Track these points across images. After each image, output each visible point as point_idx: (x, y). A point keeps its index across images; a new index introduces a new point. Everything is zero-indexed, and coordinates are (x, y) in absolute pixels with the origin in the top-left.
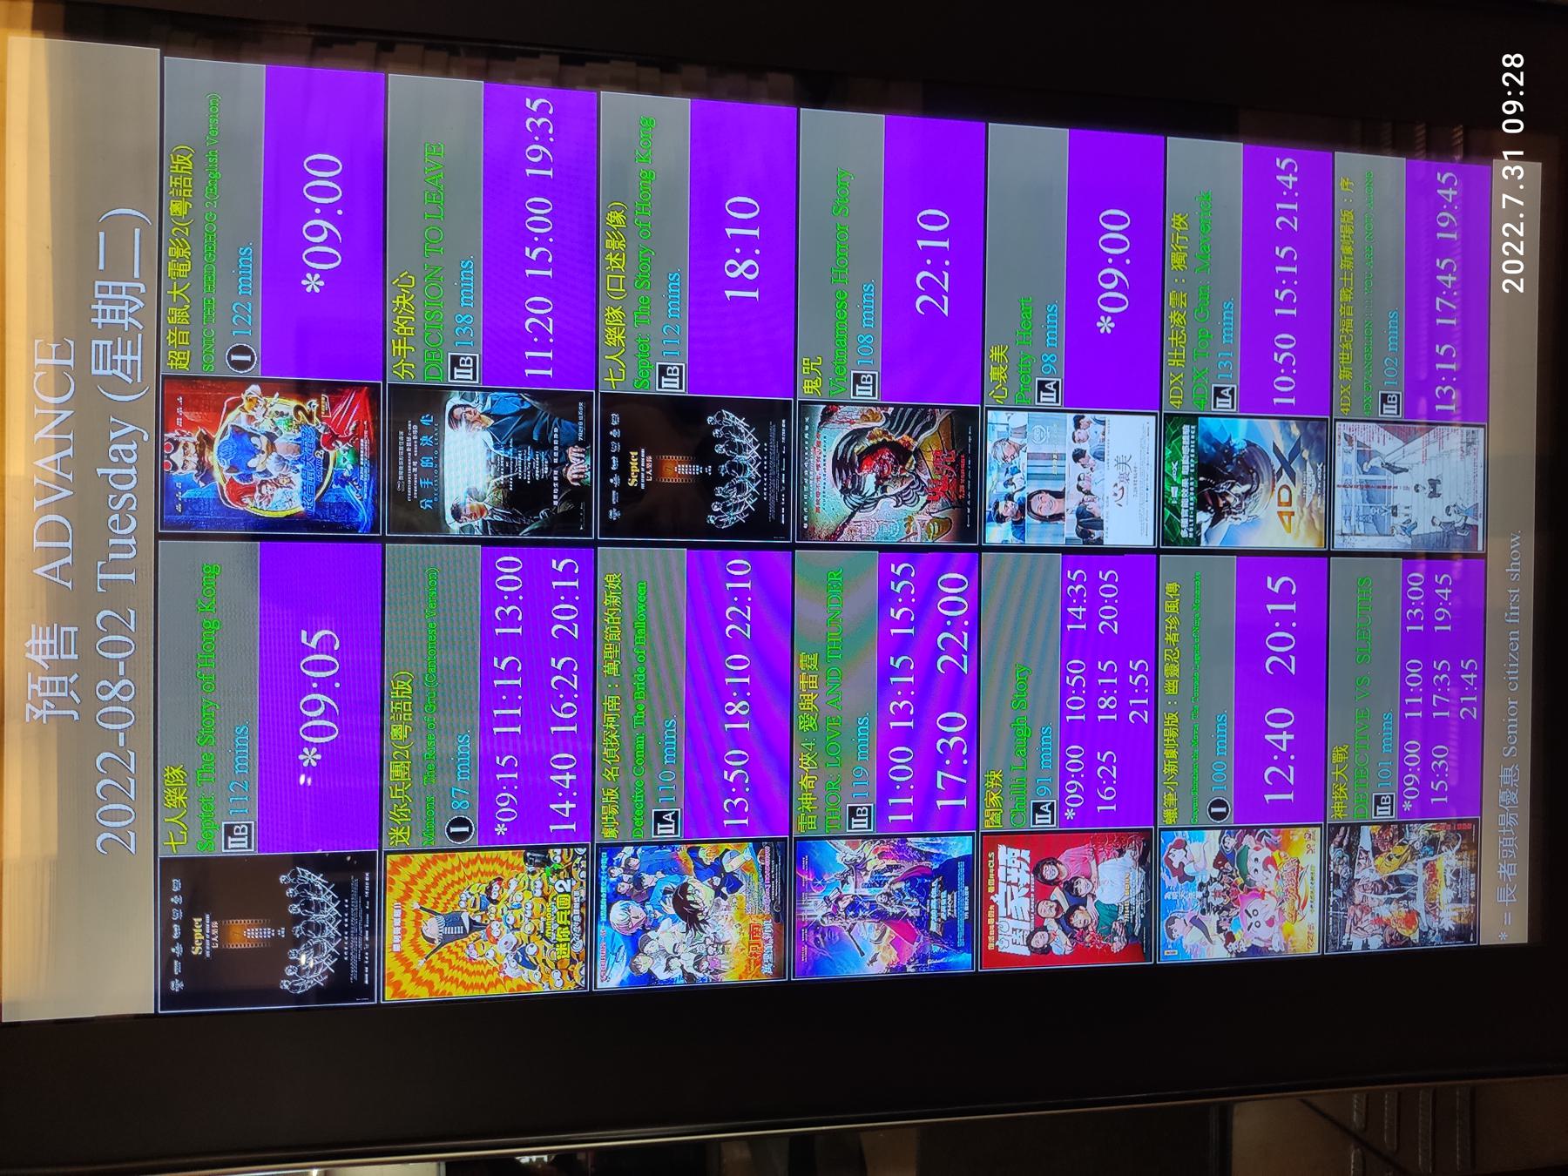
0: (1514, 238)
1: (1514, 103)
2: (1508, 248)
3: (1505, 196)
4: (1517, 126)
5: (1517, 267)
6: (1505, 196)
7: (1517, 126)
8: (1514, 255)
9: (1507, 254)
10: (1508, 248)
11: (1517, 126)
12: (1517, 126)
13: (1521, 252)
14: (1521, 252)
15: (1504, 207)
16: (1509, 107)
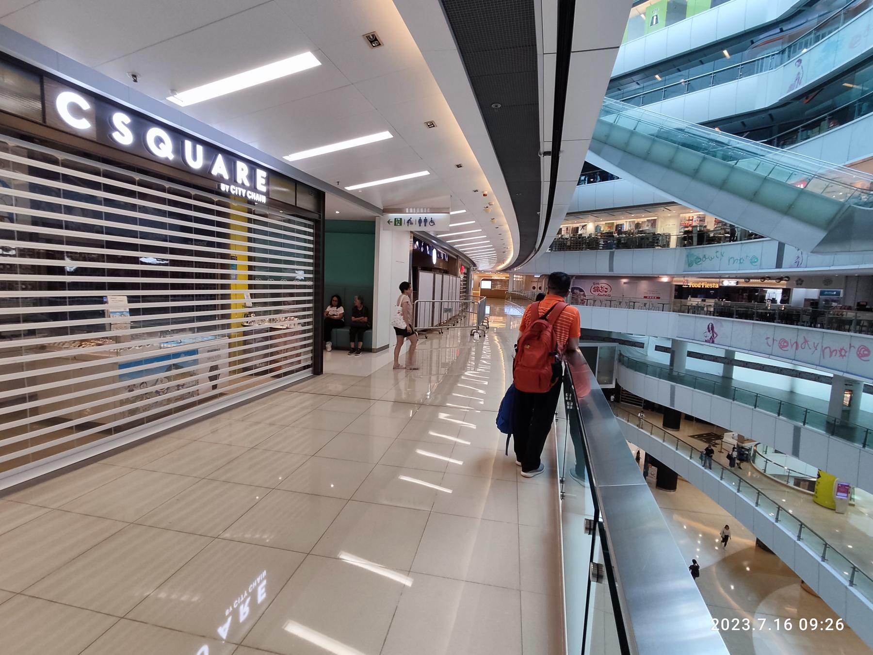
0: (742, 624)
1: (816, 625)
2: (736, 622)
3: (765, 620)
4: (803, 627)
5: (725, 627)
6: (765, 620)
7: (803, 627)
8: (732, 625)
9: (733, 621)
10: (736, 622)
11: (803, 626)
12: (803, 626)
13: (733, 629)
14: (733, 629)
15: (759, 619)
16: (814, 622)
